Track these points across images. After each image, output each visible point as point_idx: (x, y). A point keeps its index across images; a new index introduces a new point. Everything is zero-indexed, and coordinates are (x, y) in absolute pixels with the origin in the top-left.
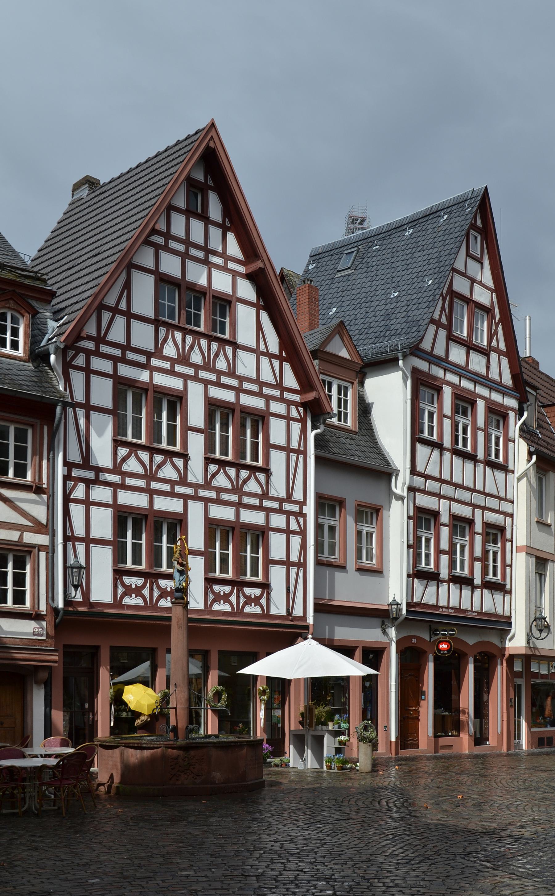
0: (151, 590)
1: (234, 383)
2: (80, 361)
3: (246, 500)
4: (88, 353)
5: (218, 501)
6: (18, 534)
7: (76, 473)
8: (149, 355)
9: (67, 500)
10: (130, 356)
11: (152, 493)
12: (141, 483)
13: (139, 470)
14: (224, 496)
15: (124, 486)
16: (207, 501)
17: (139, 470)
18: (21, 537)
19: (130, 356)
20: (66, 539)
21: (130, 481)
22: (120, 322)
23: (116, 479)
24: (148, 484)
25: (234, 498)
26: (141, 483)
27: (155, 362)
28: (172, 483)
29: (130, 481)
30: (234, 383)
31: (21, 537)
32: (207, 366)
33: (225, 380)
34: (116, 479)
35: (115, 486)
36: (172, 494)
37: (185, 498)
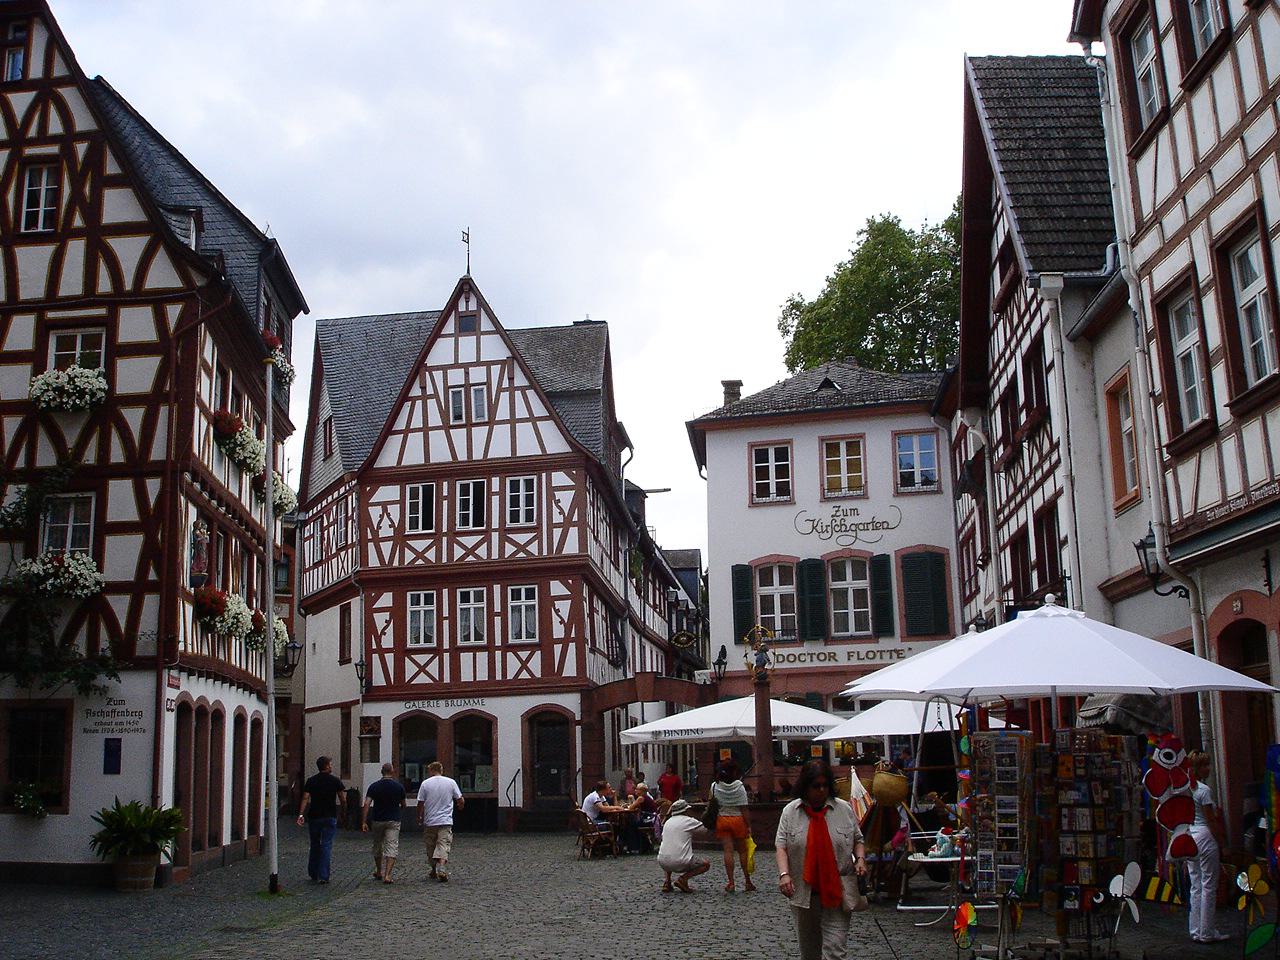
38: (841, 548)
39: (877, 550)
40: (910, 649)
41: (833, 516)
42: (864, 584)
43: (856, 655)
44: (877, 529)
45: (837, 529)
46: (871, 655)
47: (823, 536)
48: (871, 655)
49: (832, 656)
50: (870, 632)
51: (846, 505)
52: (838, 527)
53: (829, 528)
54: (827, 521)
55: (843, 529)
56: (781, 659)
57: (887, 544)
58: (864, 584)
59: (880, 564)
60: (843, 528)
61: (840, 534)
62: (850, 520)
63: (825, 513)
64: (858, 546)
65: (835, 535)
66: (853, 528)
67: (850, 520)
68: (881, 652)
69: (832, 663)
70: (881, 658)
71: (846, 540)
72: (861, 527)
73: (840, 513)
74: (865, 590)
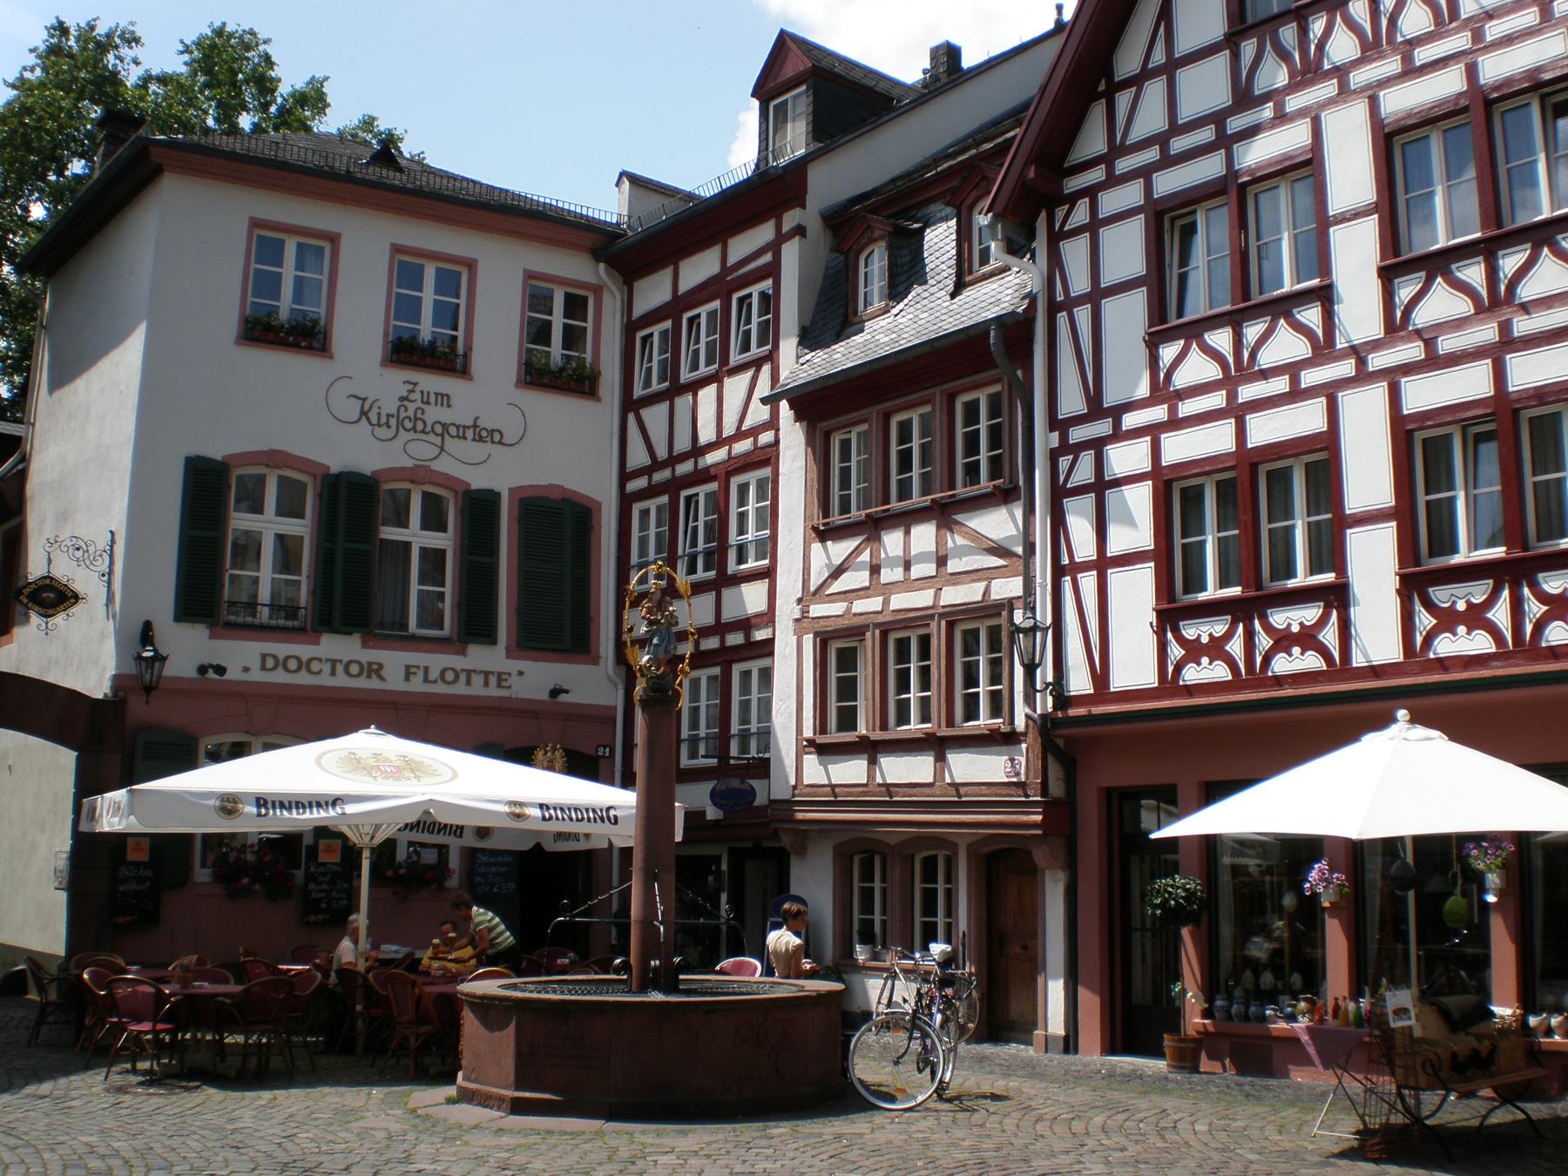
0: (1250, 636)
1: (1460, 41)
2: (1081, 215)
3: (1523, 326)
4: (1092, 192)
5: (1434, 361)
6: (981, 586)
7: (1078, 434)
8: (1217, 118)
9: (1059, 494)
10: (1178, 144)
11: (1238, 413)
12: (1217, 400)
13: (1212, 372)
14: (1446, 344)
15: (1175, 423)
16: (1393, 377)
17: (1212, 372)
18: (987, 592)
19: (1178, 144)
20: (1058, 571)
21: (1187, 408)
22: (1155, 91)
23: (1159, 413)
24: (1232, 396)
25: (1487, 333)
26: (1217, 400)
27: (1235, 124)
28: (1292, 369)
29: (1187, 408)
30: (1460, 41)
31: (987, 592)
32: (1371, 49)
33: (1423, 55)
34: (1159, 413)
35: (1153, 431)
36: (1296, 394)
37: (1330, 393)
38: (409, 463)
39: (478, 480)
40: (521, 673)
41: (402, 399)
42: (442, 541)
43: (421, 673)
44: (481, 439)
45: (408, 425)
46: (450, 676)
47: (383, 432)
48: (450, 676)
49: (374, 670)
50: (447, 630)
51: (431, 382)
52: (406, 421)
53: (393, 422)
54: (390, 406)
55: (416, 424)
56: (270, 663)
57: (500, 473)
58: (442, 541)
59: (480, 507)
60: (420, 426)
61: (412, 435)
62: (433, 414)
63: (390, 385)
64: (444, 466)
65: (404, 436)
66: (439, 429)
67: (433, 414)
68: (469, 672)
69: (374, 684)
70: (468, 683)
71: (422, 450)
72: (453, 431)
73: (416, 396)
74: (443, 553)
